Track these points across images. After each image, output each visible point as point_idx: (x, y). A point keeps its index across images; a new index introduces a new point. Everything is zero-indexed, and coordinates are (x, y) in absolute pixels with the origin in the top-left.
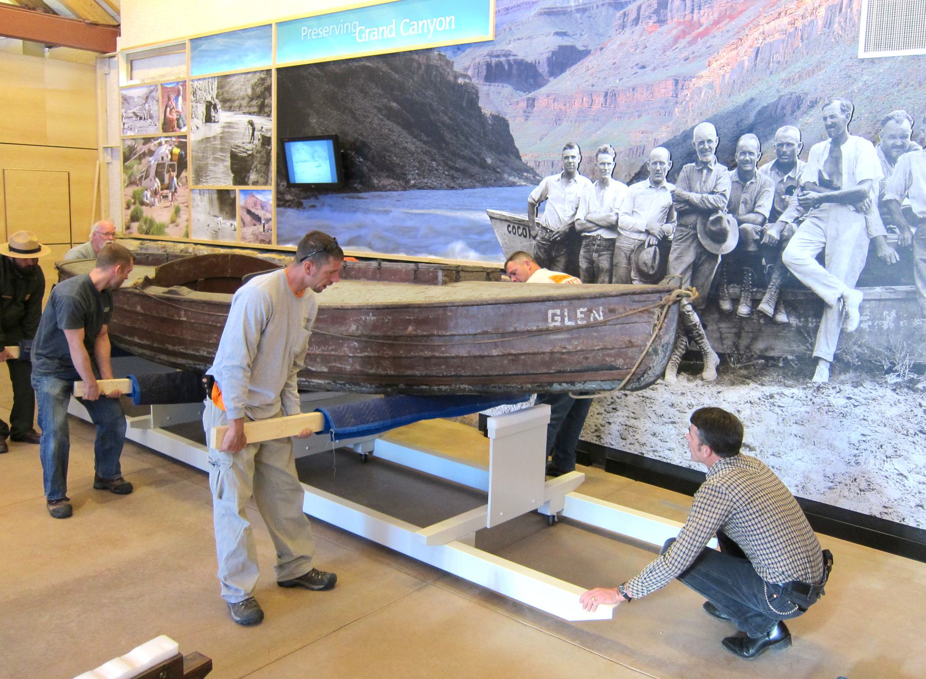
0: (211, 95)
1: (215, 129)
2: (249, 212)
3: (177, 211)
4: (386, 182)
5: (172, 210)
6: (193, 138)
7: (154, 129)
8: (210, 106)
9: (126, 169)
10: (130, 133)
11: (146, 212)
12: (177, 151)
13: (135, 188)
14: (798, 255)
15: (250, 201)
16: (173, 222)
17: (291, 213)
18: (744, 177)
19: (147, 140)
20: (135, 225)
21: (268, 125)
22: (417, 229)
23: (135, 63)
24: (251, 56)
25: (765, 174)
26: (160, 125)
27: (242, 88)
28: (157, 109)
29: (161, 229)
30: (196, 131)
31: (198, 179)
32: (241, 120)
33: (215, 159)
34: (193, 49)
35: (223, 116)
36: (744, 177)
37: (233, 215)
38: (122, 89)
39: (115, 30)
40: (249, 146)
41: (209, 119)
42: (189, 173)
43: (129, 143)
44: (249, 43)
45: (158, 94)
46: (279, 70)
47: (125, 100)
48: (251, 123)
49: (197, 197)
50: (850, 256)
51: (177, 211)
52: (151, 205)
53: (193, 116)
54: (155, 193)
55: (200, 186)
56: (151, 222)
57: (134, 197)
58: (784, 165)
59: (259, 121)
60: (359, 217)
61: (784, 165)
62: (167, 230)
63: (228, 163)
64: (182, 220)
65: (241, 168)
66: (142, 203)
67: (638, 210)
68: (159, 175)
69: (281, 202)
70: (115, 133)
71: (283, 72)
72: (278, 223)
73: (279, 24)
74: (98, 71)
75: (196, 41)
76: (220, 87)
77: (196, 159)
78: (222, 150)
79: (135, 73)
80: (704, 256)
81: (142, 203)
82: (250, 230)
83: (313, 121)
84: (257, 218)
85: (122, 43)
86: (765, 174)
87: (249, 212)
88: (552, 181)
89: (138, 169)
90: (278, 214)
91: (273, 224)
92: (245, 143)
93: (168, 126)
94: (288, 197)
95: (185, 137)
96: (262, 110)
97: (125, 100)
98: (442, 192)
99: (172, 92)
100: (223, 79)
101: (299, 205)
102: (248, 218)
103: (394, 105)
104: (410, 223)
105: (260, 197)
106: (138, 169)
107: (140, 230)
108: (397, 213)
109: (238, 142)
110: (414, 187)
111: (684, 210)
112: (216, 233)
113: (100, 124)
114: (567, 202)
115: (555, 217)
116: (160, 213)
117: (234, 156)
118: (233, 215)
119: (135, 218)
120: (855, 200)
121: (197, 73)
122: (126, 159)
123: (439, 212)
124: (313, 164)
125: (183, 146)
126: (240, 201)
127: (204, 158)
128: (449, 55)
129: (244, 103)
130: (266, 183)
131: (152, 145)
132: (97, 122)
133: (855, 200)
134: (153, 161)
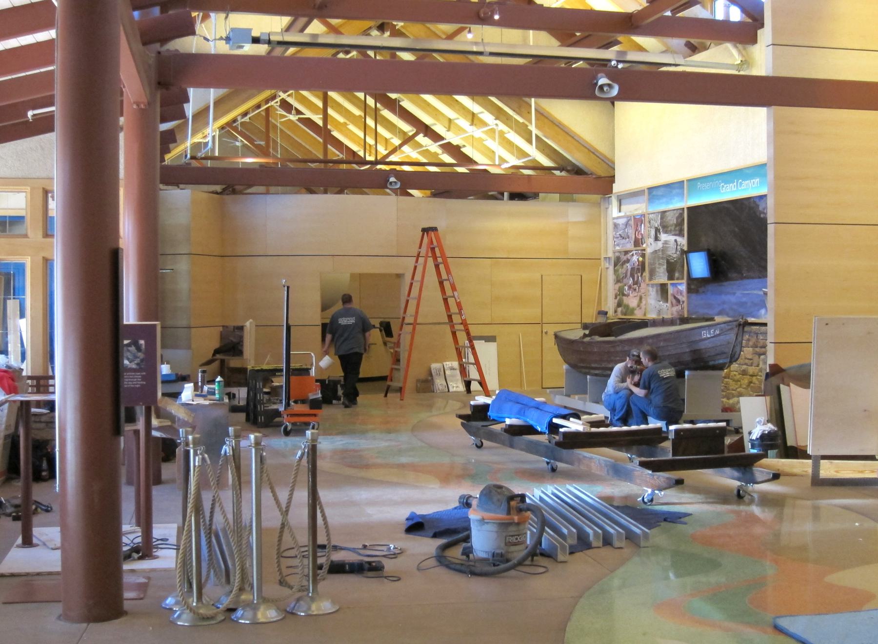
0: (657, 224)
1: (660, 245)
2: (675, 297)
3: (641, 298)
4: (734, 275)
5: (638, 298)
6: (649, 251)
7: (630, 246)
8: (657, 231)
9: (615, 271)
10: (618, 248)
11: (626, 300)
12: (641, 259)
13: (620, 284)
15: (676, 290)
16: (638, 306)
17: (694, 296)
19: (626, 253)
20: (619, 309)
21: (683, 241)
22: (746, 303)
23: (623, 201)
24: (676, 199)
26: (632, 242)
27: (672, 219)
28: (631, 231)
29: (632, 311)
30: (650, 246)
31: (651, 279)
32: (671, 238)
33: (660, 264)
34: (650, 193)
35: (663, 237)
37: (667, 301)
38: (614, 219)
39: (612, 179)
40: (675, 256)
41: (657, 239)
42: (646, 274)
43: (617, 254)
44: (674, 192)
45: (632, 222)
46: (688, 208)
47: (616, 226)
48: (676, 241)
49: (650, 289)
51: (641, 298)
52: (628, 295)
53: (649, 236)
54: (630, 287)
55: (652, 282)
56: (627, 307)
57: (619, 290)
59: (679, 239)
60: (724, 298)
62: (636, 312)
63: (665, 267)
64: (643, 305)
65: (672, 269)
66: (624, 295)
68: (632, 276)
69: (690, 290)
70: (610, 248)
71: (690, 209)
72: (689, 304)
73: (689, 181)
74: (602, 207)
75: (651, 189)
76: (662, 218)
77: (650, 264)
78: (662, 258)
79: (622, 207)
81: (624, 295)
82: (675, 309)
83: (703, 239)
84: (678, 301)
85: (617, 188)
87: (675, 297)
89: (621, 271)
90: (688, 298)
91: (685, 304)
92: (673, 253)
93: (637, 243)
94: (693, 287)
95: (644, 250)
96: (681, 234)
97: (616, 226)
98: (756, 281)
99: (638, 221)
100: (663, 213)
101: (697, 292)
102: (674, 301)
103: (736, 229)
104: (744, 299)
105: (680, 287)
106: (621, 271)
107: (622, 312)
108: (738, 293)
109: (669, 253)
110: (747, 278)
112: (659, 312)
113: (602, 242)
116: (632, 301)
117: (668, 262)
118: (667, 301)
119: (619, 305)
121: (651, 210)
122: (615, 265)
123: (755, 292)
124: (699, 265)
125: (643, 256)
126: (671, 290)
127: (654, 264)
128: (757, 200)
129: (673, 228)
130: (683, 279)
131: (629, 256)
132: (600, 242)
134: (629, 266)
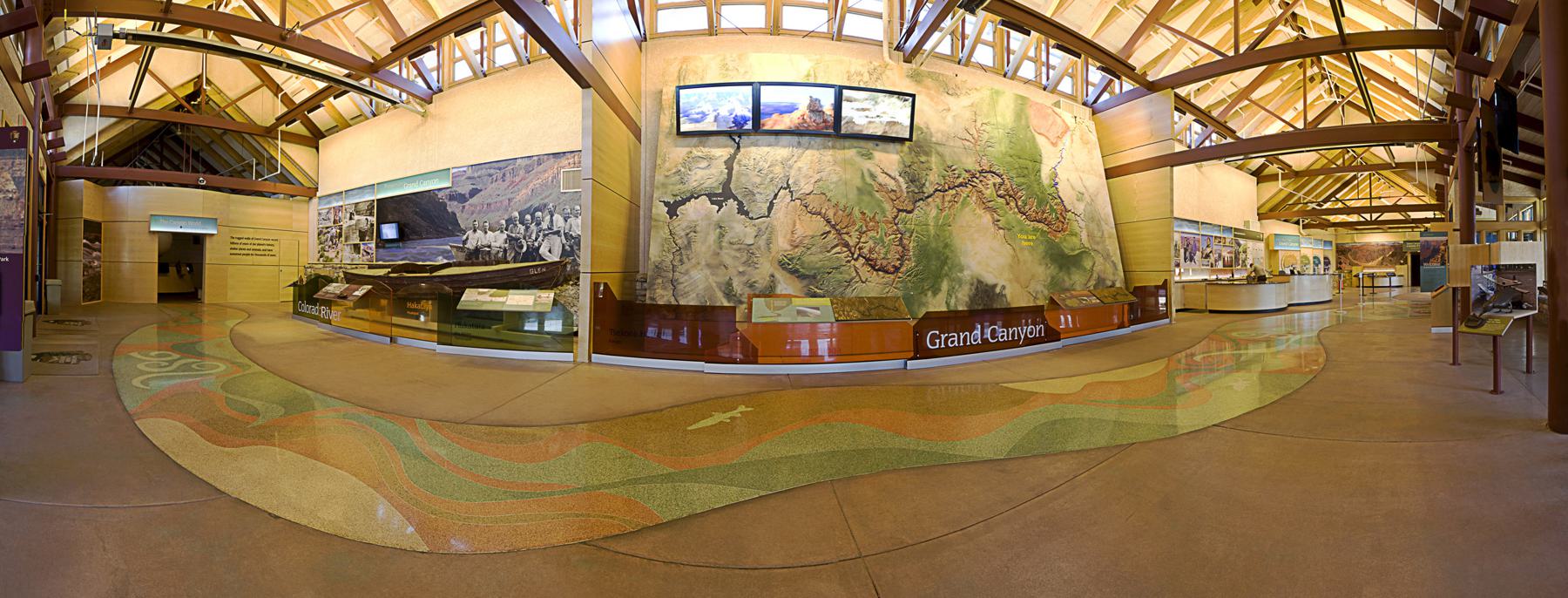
14: (543, 250)
18: (527, 228)
25: (533, 226)
36: (527, 228)
50: (558, 251)
58: (538, 224)
61: (538, 224)
67: (497, 240)
80: (517, 254)
86: (533, 226)
88: (470, 232)
111: (510, 239)
114: (474, 239)
115: (471, 245)
120: (558, 233)
133: (558, 233)
